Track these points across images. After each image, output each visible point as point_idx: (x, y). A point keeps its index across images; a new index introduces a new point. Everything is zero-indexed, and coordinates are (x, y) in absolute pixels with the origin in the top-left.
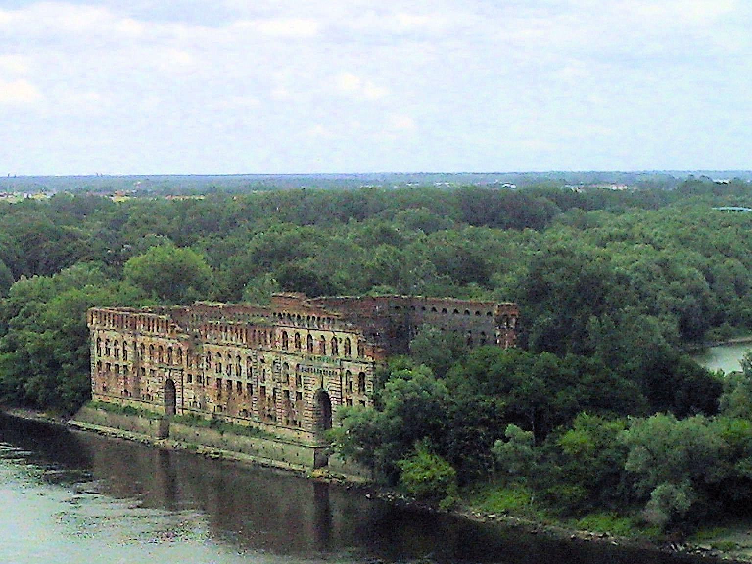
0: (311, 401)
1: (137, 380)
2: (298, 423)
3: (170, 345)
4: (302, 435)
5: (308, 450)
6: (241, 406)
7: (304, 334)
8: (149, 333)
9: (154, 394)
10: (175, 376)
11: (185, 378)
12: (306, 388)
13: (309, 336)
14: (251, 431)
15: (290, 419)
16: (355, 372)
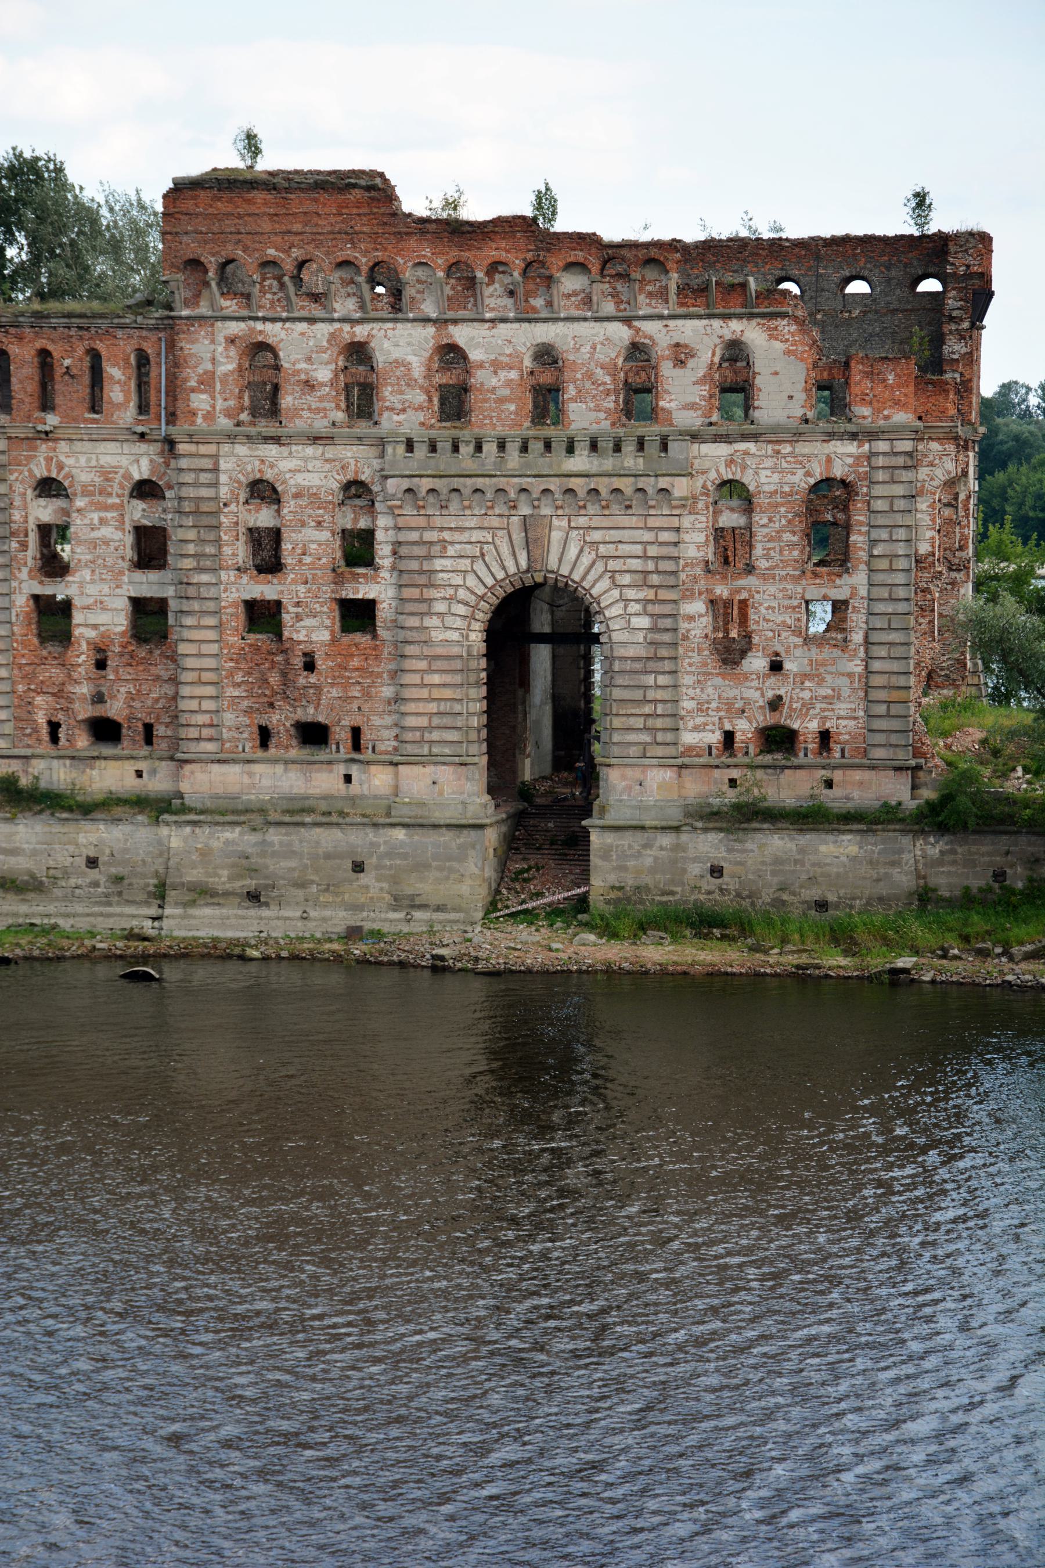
0: (457, 630)
2: (341, 735)
4: (376, 781)
5: (446, 837)
7: (403, 347)
12: (415, 580)
13: (451, 354)
16: (777, 475)
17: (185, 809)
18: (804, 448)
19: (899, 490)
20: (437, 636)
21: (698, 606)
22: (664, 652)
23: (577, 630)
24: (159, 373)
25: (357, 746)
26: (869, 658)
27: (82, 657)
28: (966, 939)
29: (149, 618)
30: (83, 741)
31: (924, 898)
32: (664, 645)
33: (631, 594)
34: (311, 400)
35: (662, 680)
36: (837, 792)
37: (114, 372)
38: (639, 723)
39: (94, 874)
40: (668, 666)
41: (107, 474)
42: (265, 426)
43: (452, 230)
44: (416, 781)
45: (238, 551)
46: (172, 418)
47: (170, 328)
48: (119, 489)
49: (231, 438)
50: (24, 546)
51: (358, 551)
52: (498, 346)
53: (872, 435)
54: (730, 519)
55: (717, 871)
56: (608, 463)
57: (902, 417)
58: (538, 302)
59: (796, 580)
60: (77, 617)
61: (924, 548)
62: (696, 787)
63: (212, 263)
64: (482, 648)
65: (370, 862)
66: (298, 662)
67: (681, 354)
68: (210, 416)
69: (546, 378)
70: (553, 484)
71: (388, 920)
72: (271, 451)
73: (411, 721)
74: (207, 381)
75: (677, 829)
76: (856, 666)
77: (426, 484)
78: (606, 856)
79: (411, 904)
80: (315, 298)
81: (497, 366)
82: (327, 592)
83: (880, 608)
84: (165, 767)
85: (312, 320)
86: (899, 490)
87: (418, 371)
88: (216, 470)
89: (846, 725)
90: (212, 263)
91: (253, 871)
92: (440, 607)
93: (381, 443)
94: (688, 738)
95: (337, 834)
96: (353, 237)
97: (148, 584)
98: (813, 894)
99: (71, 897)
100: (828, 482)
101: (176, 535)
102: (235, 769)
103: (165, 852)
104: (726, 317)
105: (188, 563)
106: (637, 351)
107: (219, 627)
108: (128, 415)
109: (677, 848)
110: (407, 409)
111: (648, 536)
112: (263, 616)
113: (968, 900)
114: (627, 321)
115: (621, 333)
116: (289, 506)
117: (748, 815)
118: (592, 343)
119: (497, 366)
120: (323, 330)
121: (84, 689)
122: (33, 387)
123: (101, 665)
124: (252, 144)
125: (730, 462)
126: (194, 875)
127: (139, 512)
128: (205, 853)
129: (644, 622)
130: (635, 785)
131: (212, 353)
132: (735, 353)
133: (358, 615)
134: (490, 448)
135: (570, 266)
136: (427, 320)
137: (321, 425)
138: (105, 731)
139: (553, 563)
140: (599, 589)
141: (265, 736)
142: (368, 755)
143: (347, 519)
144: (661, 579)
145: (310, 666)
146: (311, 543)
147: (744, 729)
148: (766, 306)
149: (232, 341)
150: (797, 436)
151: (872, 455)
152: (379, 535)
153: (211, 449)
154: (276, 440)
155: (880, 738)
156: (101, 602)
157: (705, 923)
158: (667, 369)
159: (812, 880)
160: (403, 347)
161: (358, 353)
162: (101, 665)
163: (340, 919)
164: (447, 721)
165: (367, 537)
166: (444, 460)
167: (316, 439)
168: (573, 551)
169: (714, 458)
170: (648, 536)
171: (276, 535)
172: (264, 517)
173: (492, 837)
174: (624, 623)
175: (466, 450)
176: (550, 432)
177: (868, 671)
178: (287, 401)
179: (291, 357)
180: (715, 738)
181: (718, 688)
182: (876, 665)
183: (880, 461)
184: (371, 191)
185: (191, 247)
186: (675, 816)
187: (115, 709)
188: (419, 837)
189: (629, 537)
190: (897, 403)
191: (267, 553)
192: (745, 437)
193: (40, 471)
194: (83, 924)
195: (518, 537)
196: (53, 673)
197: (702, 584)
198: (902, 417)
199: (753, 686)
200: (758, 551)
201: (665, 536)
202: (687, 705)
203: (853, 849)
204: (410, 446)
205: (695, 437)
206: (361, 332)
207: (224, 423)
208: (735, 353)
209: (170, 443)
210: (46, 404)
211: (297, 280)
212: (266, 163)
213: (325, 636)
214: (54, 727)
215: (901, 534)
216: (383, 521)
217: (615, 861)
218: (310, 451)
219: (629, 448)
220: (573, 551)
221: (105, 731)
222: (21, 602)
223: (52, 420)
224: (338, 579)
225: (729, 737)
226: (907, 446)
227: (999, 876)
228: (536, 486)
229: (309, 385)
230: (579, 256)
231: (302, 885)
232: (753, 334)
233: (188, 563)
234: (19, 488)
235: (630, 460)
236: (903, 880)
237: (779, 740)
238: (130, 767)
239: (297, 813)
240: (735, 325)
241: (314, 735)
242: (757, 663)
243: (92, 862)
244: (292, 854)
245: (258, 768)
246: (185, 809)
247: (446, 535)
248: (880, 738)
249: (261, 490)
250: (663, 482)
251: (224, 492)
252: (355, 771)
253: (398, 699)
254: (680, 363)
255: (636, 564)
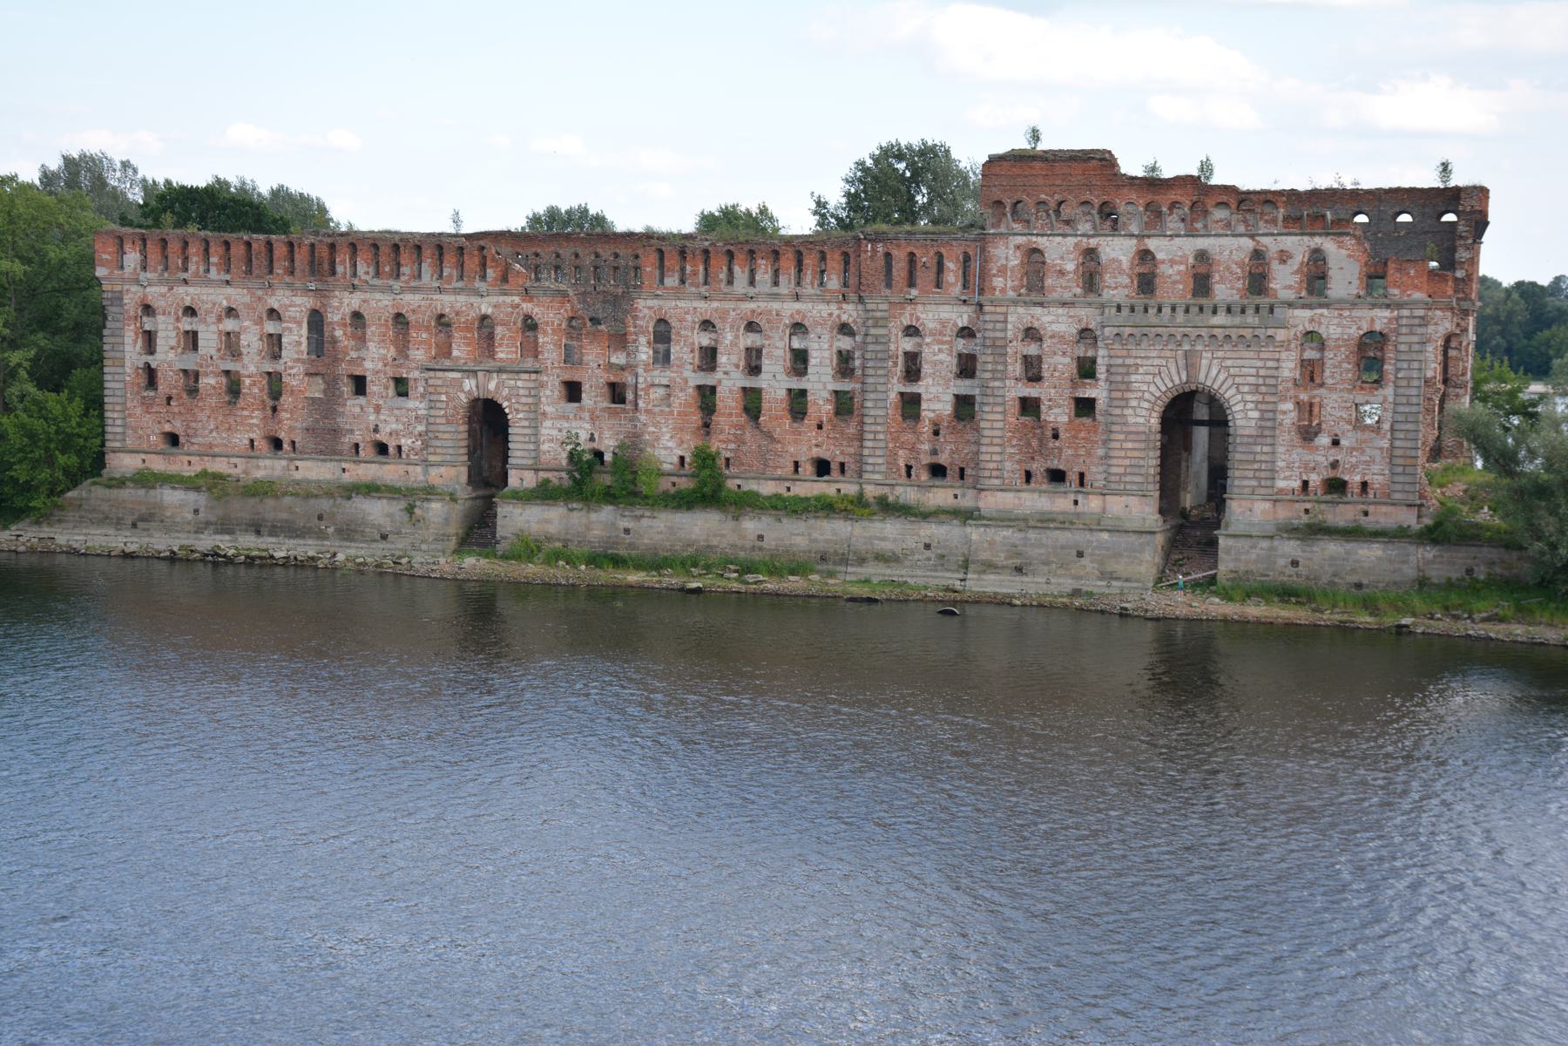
0: (1144, 416)
1: (327, 407)
2: (1073, 477)
3: (486, 309)
4: (1093, 504)
5: (1133, 538)
6: (807, 444)
7: (1118, 250)
8: (397, 285)
9: (406, 442)
10: (506, 390)
11: (552, 391)
12: (1121, 387)
13: (1145, 255)
14: (856, 507)
15: (1038, 467)
16: (1340, 328)
17: (981, 517)
18: (1357, 313)
19: (1415, 339)
20: (1131, 420)
21: (1289, 406)
22: (1267, 433)
23: (1219, 421)
24: (976, 266)
25: (1082, 484)
26: (1393, 439)
27: (926, 428)
28: (1447, 608)
29: (965, 407)
30: (924, 476)
31: (1422, 583)
32: (1268, 428)
33: (1249, 397)
34: (1063, 281)
35: (1266, 449)
36: (1370, 518)
37: (950, 265)
38: (1251, 474)
39: (928, 553)
40: (1269, 440)
41: (943, 323)
42: (1034, 297)
43: (1151, 183)
44: (1116, 505)
45: (1016, 368)
46: (982, 291)
47: (983, 240)
48: (950, 332)
49: (1015, 303)
50: (896, 364)
51: (1086, 370)
52: (1173, 251)
53: (1399, 306)
54: (1310, 354)
55: (1295, 563)
56: (1237, 320)
57: (1418, 295)
58: (1199, 225)
59: (1349, 391)
60: (924, 406)
61: (1430, 374)
62: (1283, 513)
63: (1008, 202)
64: (1159, 427)
65: (1087, 552)
66: (1049, 433)
67: (1284, 257)
68: (1003, 291)
69: (1202, 270)
70: (1204, 332)
71: (1098, 586)
72: (1038, 310)
73: (1114, 470)
74: (1003, 271)
75: (1272, 537)
76: (1385, 444)
77: (1128, 331)
78: (1228, 552)
79: (1111, 577)
80: (1067, 222)
81: (1172, 262)
82: (1067, 393)
83: (1401, 409)
84: (971, 493)
85: (1064, 236)
86: (1415, 339)
87: (1126, 265)
88: (1006, 321)
89: (1377, 480)
90: (1008, 202)
91: (1019, 554)
92: (1134, 403)
93: (1102, 307)
94: (1281, 484)
95: (1068, 534)
96: (1090, 187)
97: (964, 387)
98: (1354, 579)
99: (914, 566)
100: (1370, 333)
101: (981, 359)
102: (1011, 495)
103: (968, 542)
104: (1312, 235)
105: (988, 375)
106: (1257, 255)
107: (1004, 412)
108: (957, 290)
109: (1271, 549)
110: (1117, 287)
111: (1260, 364)
112: (1029, 406)
113: (1450, 585)
114: (1252, 237)
115: (1248, 244)
116: (1047, 343)
117: (1315, 531)
118: (1230, 249)
119: (1172, 262)
120: (1071, 241)
121: (926, 447)
122: (904, 274)
123: (936, 433)
124: (1035, 135)
125: (1312, 320)
126: (985, 556)
127: (961, 345)
128: (992, 543)
129: (1256, 414)
130: (1248, 510)
131: (1006, 254)
132: (1317, 256)
133: (1085, 407)
134: (1167, 310)
135: (1219, 204)
136: (1133, 235)
137: (1067, 296)
138: (938, 471)
139: (1202, 378)
140: (1229, 395)
141: (1028, 476)
142: (1088, 489)
143: (1081, 351)
144: (1267, 389)
145: (1056, 436)
146: (1059, 364)
147: (1315, 479)
148: (1340, 227)
149: (1018, 247)
150: (1354, 305)
151: (1399, 318)
152: (1099, 361)
153: (1004, 309)
154: (1041, 304)
155: (1399, 487)
156: (937, 396)
157: (1286, 594)
158: (1275, 265)
159: (1353, 570)
160: (1118, 250)
161: (1091, 253)
162: (936, 433)
163: (1068, 584)
164: (1136, 470)
165: (1093, 361)
166: (1139, 317)
167: (1064, 304)
168: (1214, 372)
169: (1302, 318)
170: (1260, 364)
171: (1039, 358)
172: (1032, 349)
173: (1160, 539)
174: (1244, 415)
175: (1152, 311)
176: (1203, 301)
177: (1392, 447)
178: (1049, 282)
179: (1052, 257)
180: (1297, 484)
181: (1299, 455)
182: (1398, 443)
183: (1404, 321)
184: (1102, 162)
185: (997, 194)
186: (1270, 529)
187: (943, 459)
188: (1116, 538)
189: (1248, 364)
190: (1416, 287)
191: (1033, 371)
192: (1321, 306)
193: (906, 322)
194: (921, 582)
195: (1181, 362)
196: (908, 437)
197: (1292, 393)
198: (1418, 295)
199: (1321, 454)
200: (1327, 373)
201: (1270, 364)
202: (1280, 464)
203: (1379, 553)
204: (1119, 308)
205: (1290, 305)
206: (1093, 242)
207: (1011, 294)
208: (1317, 256)
209: (980, 306)
210: (912, 284)
211: (1057, 212)
212: (1041, 147)
213: (1065, 419)
214: (909, 468)
215: (1416, 365)
216: (1101, 352)
217: (1233, 555)
218: (1060, 311)
219: (1250, 311)
220: (1214, 372)
221: (938, 471)
222: (893, 396)
223: (914, 292)
224: (1074, 385)
225: (1305, 484)
226: (1421, 313)
227: (1469, 571)
228: (1194, 333)
229: (1062, 273)
230: (1225, 198)
231: (1047, 563)
232: (1328, 245)
233: (988, 375)
234: (894, 331)
235: (1251, 318)
236: (1410, 572)
237: (1336, 486)
238: (950, 492)
239: (1045, 521)
240: (1318, 240)
241: (1057, 476)
242: (1324, 440)
243: (927, 546)
244: (1041, 545)
245: (1023, 495)
246: (981, 517)
247: (1139, 361)
248: (1399, 487)
249: (1032, 334)
250: (1270, 332)
251: (1010, 334)
252: (1080, 498)
253: (1107, 457)
254: (1283, 262)
255: (1252, 380)
